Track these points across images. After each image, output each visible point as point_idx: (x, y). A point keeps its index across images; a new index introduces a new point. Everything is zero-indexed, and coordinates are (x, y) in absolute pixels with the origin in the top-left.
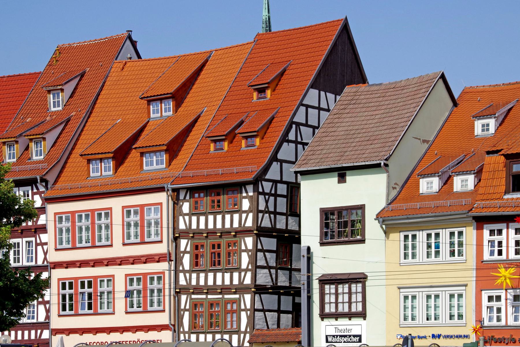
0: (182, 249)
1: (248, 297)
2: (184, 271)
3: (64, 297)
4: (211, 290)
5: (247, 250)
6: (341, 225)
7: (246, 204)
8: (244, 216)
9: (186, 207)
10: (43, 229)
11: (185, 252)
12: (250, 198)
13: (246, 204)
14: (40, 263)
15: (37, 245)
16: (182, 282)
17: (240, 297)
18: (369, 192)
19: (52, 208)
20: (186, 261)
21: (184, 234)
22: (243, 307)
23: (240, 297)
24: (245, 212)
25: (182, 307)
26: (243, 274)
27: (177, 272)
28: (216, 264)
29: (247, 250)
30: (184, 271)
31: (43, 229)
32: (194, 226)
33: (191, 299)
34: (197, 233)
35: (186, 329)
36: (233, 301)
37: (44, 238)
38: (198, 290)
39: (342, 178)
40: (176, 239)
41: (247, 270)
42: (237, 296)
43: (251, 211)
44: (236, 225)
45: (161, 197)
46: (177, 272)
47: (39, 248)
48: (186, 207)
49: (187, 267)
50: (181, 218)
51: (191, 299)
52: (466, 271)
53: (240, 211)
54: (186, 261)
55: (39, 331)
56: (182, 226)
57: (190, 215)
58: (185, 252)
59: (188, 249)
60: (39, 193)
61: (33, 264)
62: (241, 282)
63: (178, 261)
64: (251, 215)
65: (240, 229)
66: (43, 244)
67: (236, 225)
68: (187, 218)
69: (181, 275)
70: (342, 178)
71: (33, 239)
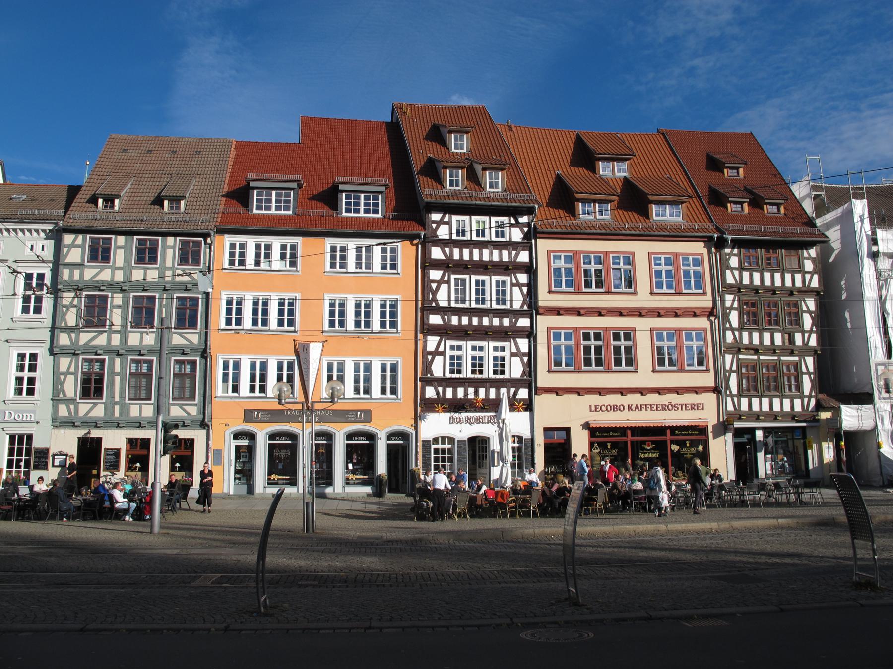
0: (728, 304)
1: (810, 360)
2: (733, 330)
3: (557, 349)
5: (809, 311)
7: (809, 266)
8: (808, 276)
11: (731, 308)
12: (813, 260)
13: (809, 266)
14: (517, 306)
15: (513, 285)
17: (800, 360)
19: (543, 246)
21: (731, 289)
22: (804, 370)
23: (800, 360)
24: (808, 272)
25: (728, 368)
26: (806, 335)
29: (809, 311)
30: (733, 330)
32: (746, 281)
33: (738, 360)
35: (734, 391)
36: (788, 364)
41: (811, 332)
42: (797, 358)
43: (816, 273)
44: (798, 284)
47: (516, 290)
48: (734, 262)
49: (735, 324)
50: (728, 272)
51: (738, 360)
53: (804, 273)
54: (734, 317)
55: (513, 390)
56: (730, 280)
57: (741, 268)
58: (731, 308)
59: (736, 305)
61: (507, 306)
62: (805, 344)
64: (816, 277)
65: (804, 289)
66: (520, 286)
68: (736, 273)
69: (729, 334)
71: (506, 279)
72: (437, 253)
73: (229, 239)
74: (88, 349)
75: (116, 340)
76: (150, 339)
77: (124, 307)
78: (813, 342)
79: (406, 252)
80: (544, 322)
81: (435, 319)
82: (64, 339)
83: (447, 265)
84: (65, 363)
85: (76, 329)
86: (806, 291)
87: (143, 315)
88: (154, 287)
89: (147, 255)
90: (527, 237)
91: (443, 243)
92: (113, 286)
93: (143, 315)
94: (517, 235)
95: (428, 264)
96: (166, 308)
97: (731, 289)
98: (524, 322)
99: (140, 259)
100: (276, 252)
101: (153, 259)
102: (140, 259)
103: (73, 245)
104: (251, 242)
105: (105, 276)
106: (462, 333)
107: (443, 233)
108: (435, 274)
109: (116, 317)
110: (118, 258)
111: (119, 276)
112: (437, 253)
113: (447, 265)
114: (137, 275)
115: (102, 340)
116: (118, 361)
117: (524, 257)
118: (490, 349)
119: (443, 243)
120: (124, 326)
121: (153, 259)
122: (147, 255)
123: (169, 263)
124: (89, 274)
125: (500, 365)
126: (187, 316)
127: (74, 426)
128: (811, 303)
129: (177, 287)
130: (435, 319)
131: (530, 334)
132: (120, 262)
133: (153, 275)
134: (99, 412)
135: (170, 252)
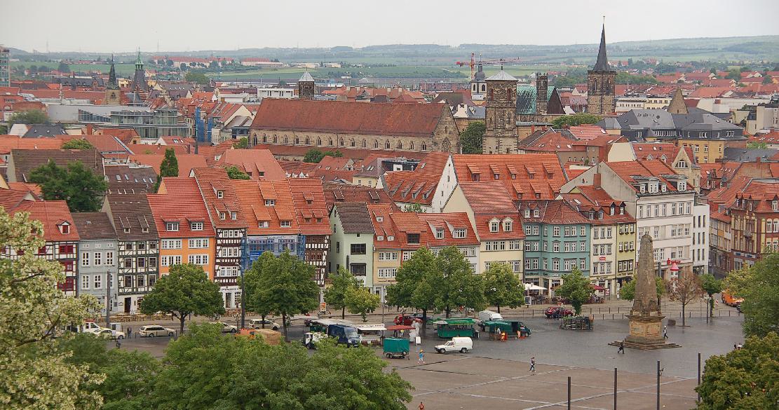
1: (324, 270)
6: (358, 249)
7: (326, 241)
13: (326, 241)
18: (367, 240)
39: (358, 236)
44: (322, 247)
53: (324, 243)
60: (242, 232)
67: (322, 247)
70: (358, 236)
73: (163, 240)
74: (126, 274)
75: (134, 271)
76: (143, 270)
77: (136, 262)
78: (325, 264)
79: (209, 242)
81: (218, 261)
82: (121, 272)
83: (223, 245)
84: (120, 277)
85: (124, 268)
87: (141, 264)
90: (244, 235)
91: (221, 239)
92: (133, 256)
94: (241, 235)
99: (140, 248)
102: (140, 248)
103: (121, 245)
105: (131, 253)
106: (225, 264)
107: (220, 236)
108: (218, 248)
111: (135, 253)
112: (219, 242)
113: (223, 245)
114: (139, 253)
115: (130, 271)
116: (134, 277)
119: (221, 239)
120: (136, 267)
122: (141, 247)
123: (148, 249)
124: (127, 253)
127: (123, 294)
130: (218, 261)
132: (135, 249)
133: (143, 252)
134: (130, 290)
135: (148, 246)
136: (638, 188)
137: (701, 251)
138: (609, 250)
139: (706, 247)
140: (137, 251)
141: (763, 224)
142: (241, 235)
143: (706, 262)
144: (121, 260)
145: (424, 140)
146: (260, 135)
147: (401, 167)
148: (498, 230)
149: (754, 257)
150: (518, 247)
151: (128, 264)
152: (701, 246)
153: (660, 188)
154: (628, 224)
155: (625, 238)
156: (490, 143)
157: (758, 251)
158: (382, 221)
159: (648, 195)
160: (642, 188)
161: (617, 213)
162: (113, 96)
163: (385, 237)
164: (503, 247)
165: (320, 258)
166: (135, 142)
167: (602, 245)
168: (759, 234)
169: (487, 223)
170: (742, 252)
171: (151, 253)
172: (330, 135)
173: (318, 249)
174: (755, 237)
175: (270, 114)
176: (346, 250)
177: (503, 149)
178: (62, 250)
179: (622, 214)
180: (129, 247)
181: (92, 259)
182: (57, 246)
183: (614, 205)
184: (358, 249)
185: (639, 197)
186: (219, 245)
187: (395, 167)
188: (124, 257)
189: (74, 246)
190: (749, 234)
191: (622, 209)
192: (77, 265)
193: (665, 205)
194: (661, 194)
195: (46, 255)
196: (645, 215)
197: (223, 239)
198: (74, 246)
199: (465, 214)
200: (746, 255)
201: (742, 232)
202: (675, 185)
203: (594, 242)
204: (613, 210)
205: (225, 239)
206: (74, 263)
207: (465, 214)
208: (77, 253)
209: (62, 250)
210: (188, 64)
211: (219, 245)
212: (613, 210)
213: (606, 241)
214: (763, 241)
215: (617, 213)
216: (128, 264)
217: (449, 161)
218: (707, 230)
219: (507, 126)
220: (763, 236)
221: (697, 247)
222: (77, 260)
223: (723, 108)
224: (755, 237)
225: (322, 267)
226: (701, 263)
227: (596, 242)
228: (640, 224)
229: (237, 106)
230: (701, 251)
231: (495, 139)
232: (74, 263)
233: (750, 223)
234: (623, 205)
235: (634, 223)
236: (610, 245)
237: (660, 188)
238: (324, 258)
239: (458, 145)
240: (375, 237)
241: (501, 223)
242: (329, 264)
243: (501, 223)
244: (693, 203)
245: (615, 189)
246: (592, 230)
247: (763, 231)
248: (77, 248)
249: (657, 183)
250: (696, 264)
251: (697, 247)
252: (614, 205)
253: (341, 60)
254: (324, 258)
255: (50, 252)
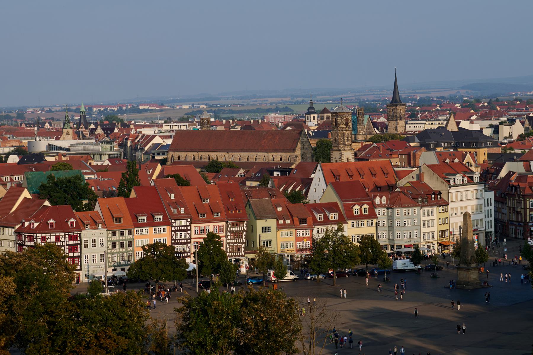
1: (244, 245)
4: (236, 243)
6: (266, 230)
7: (245, 225)
9: (230, 226)
10: (190, 230)
16: (228, 241)
18: (272, 223)
19: (193, 225)
20: (229, 237)
21: (229, 231)
27: (227, 240)
28: (237, 238)
31: (190, 230)
34: (233, 231)
37: (189, 232)
38: (232, 243)
40: (227, 233)
45: (224, 224)
46: (227, 240)
48: (230, 226)
52: (293, 238)
63: (227, 237)
72: (173, 229)
75: (118, 250)
79: (168, 228)
80: (193, 241)
86: (244, 231)
88: (124, 240)
89: (122, 234)
90: (190, 224)
91: (174, 227)
92: (117, 241)
93: (122, 245)
94: (188, 224)
95: (172, 231)
96: (126, 245)
97: (229, 231)
98: (189, 241)
100: (144, 230)
101: (123, 235)
104: (139, 229)
105: (115, 239)
107: (174, 225)
108: (173, 233)
109: (117, 246)
110: (117, 235)
111: (118, 239)
112: (173, 229)
114: (121, 238)
115: (116, 251)
117: (189, 228)
118: (183, 246)
119: (174, 227)
121: (123, 235)
125: (184, 249)
126: (130, 245)
128: (245, 233)
129: (128, 239)
131: (190, 243)
133: (124, 238)
136: (449, 182)
137: (490, 222)
138: (433, 224)
139: (493, 219)
140: (119, 237)
141: (528, 202)
142: (188, 224)
143: (493, 230)
144: (109, 243)
145: (289, 154)
146: (176, 155)
147: (279, 174)
148: (359, 213)
149: (522, 224)
150: (372, 224)
151: (114, 246)
152: (490, 219)
153: (463, 180)
154: (443, 206)
155: (442, 215)
156: (335, 155)
157: (526, 220)
158: (281, 210)
159: (455, 185)
160: (452, 180)
161: (436, 198)
162: (68, 133)
163: (284, 221)
164: (363, 225)
165: (241, 237)
166: (90, 163)
167: (428, 221)
168: (525, 209)
169: (352, 208)
170: (515, 221)
171: (129, 238)
172: (224, 153)
173: (239, 231)
174: (523, 212)
175: (182, 141)
176: (259, 231)
177: (344, 160)
178: (71, 238)
179: (439, 199)
180: (114, 234)
181: (90, 244)
182: (67, 236)
183: (434, 194)
184: (266, 230)
185: (450, 187)
186: (173, 231)
187: (275, 174)
188: (110, 241)
189: (79, 235)
190: (519, 210)
191: (439, 196)
192: (81, 248)
193: (466, 192)
194: (463, 185)
195: (60, 242)
196: (454, 200)
197: (176, 226)
198: (79, 235)
199: (336, 203)
200: (517, 224)
201: (514, 208)
202: (472, 178)
203: (423, 219)
204: (433, 197)
205: (178, 226)
206: (79, 246)
207: (336, 203)
208: (80, 240)
209: (71, 238)
210: (102, 109)
211: (173, 231)
212: (433, 197)
213: (431, 218)
214: (528, 213)
215: (436, 198)
216: (114, 246)
217: (319, 168)
218: (492, 208)
219: (347, 143)
220: (528, 210)
221: (487, 219)
222: (80, 244)
223: (476, 127)
224: (523, 212)
225: (243, 243)
226: (490, 230)
227: (424, 218)
228: (451, 205)
229: (154, 137)
230: (490, 222)
231: (339, 152)
232: (79, 246)
233: (519, 202)
234: (440, 193)
235: (447, 204)
236: (433, 220)
237: (463, 180)
238: (244, 237)
239: (312, 156)
240: (278, 221)
241: (361, 209)
242: (247, 240)
243: (361, 209)
244: (484, 190)
245: (433, 182)
246: (421, 210)
247: (528, 207)
248: (80, 236)
249: (461, 178)
250: (487, 230)
251: (487, 219)
252: (434, 193)
253: (205, 102)
254: (244, 237)
255: (63, 240)
